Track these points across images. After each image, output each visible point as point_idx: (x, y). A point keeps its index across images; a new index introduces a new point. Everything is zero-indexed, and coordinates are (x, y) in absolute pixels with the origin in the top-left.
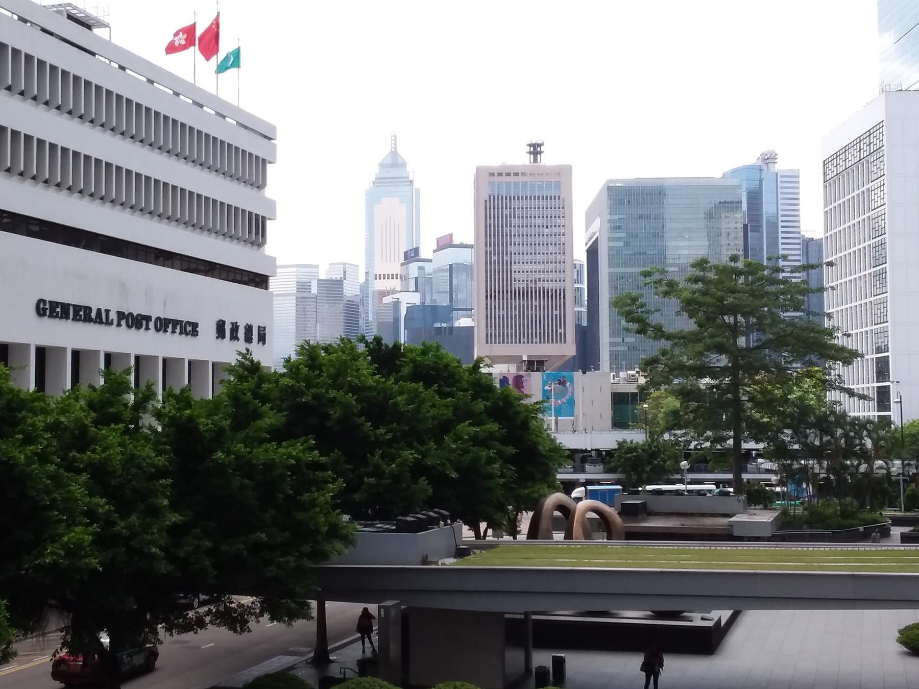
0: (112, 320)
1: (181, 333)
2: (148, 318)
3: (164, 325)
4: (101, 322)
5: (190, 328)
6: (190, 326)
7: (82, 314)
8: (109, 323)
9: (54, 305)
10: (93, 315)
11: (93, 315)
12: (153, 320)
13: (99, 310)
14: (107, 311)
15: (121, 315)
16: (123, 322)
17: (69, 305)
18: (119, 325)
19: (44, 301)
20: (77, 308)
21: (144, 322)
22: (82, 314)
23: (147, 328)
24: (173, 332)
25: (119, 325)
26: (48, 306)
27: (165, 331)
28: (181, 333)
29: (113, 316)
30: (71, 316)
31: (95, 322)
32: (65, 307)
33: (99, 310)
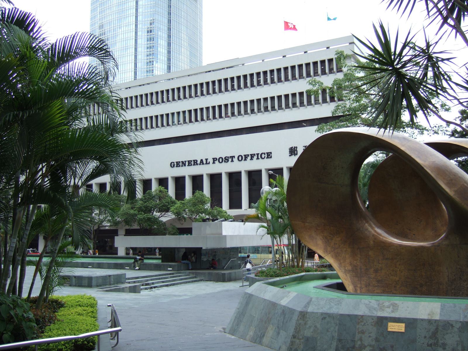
0: (209, 162)
1: (258, 158)
2: (233, 157)
4: (203, 164)
5: (266, 156)
6: (265, 155)
10: (199, 162)
11: (199, 162)
12: (236, 157)
13: (202, 160)
14: (207, 160)
15: (214, 160)
17: (185, 161)
19: (174, 163)
21: (230, 160)
23: (232, 161)
24: (251, 159)
25: (214, 163)
26: (175, 164)
27: (245, 160)
28: (258, 158)
29: (211, 161)
31: (200, 164)
33: (202, 160)
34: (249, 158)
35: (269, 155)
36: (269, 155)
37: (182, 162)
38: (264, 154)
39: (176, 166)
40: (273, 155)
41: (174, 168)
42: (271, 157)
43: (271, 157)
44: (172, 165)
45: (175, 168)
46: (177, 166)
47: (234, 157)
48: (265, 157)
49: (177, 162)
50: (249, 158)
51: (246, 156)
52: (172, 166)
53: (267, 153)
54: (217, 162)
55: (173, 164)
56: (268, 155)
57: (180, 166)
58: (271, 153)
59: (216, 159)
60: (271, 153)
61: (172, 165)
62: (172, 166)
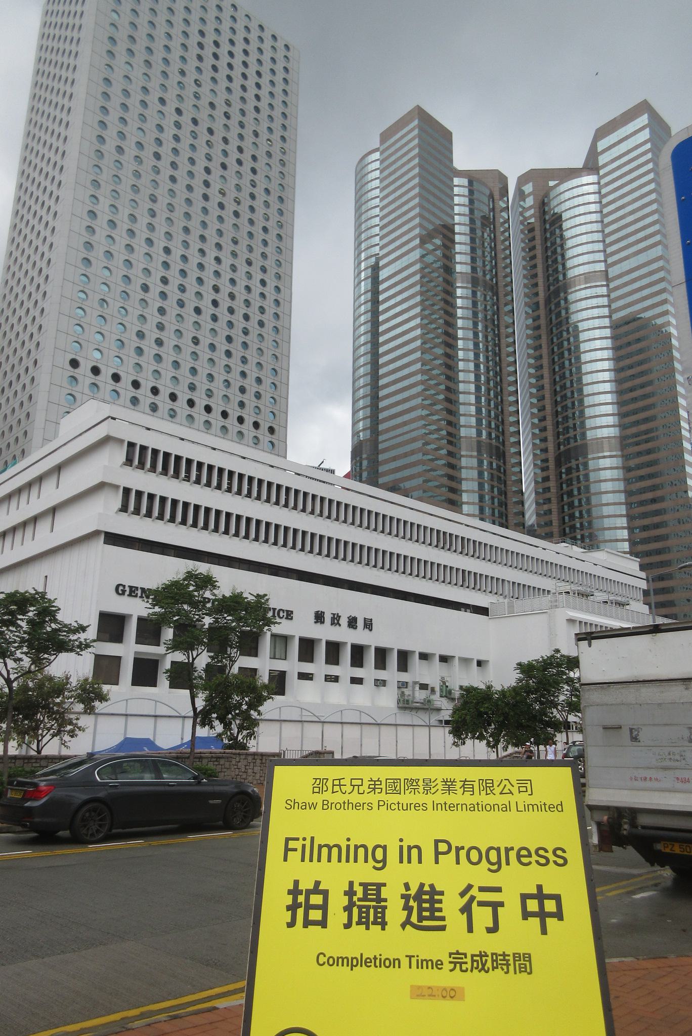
5: (285, 614)
19: (124, 586)
26: (127, 589)
37: (143, 590)
38: (283, 611)
39: (127, 593)
41: (122, 597)
42: (292, 619)
43: (292, 619)
44: (120, 590)
45: (125, 598)
46: (130, 595)
49: (131, 587)
52: (120, 592)
53: (287, 611)
55: (121, 588)
56: (288, 615)
57: (136, 596)
58: (292, 612)
60: (292, 612)
61: (120, 590)
62: (120, 592)
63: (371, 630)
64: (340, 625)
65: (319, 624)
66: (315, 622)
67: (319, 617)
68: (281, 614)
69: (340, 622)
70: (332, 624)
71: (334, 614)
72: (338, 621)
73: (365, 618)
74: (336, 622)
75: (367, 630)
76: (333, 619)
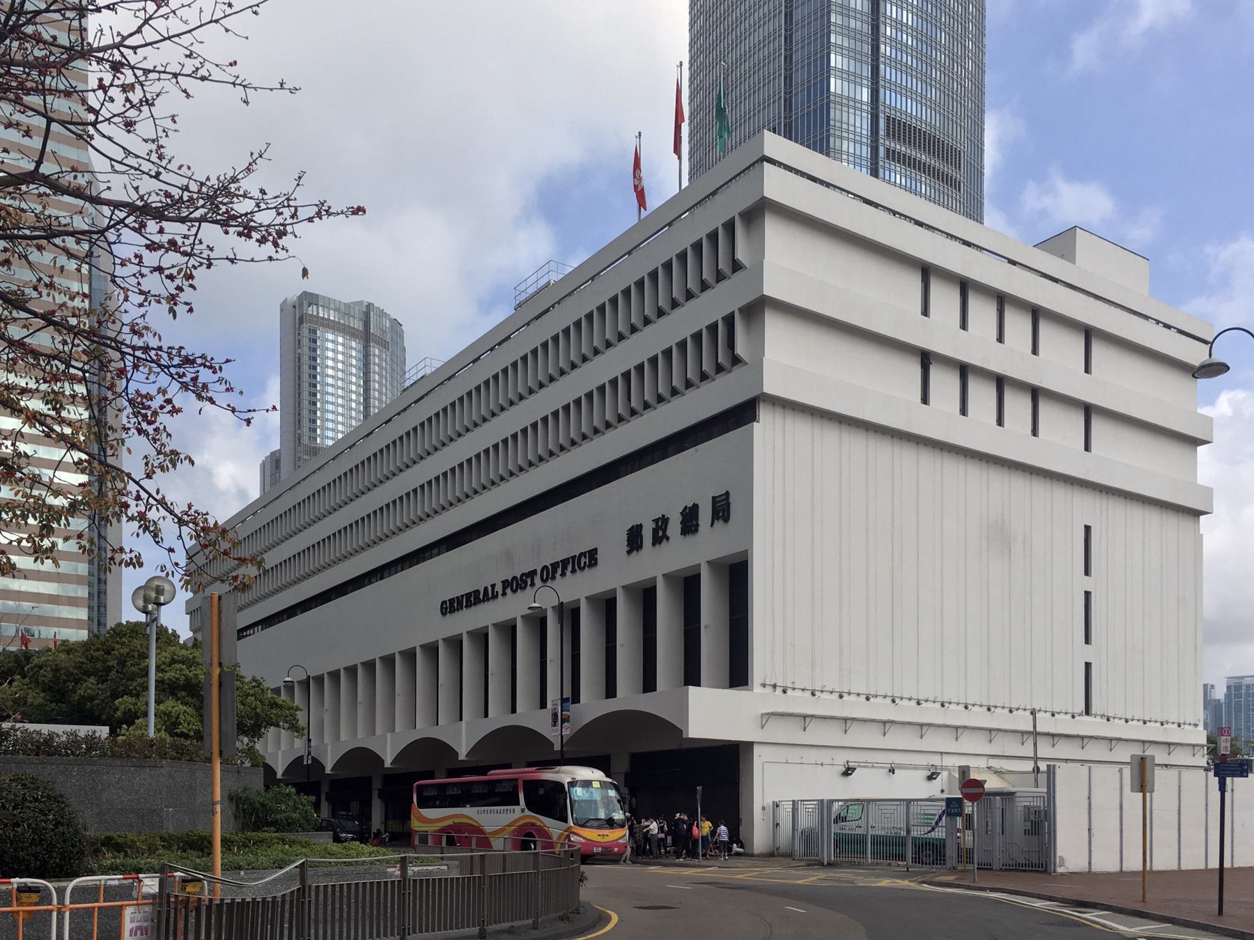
1: (573, 571)
2: (532, 574)
3: (550, 572)
6: (585, 557)
7: (473, 599)
8: (495, 597)
9: (451, 601)
10: (481, 597)
11: (481, 597)
14: (493, 586)
15: (506, 584)
16: (508, 591)
17: (462, 596)
18: (504, 594)
20: (468, 595)
22: (473, 599)
23: (533, 584)
24: (563, 574)
27: (553, 578)
29: (499, 588)
30: (464, 605)
31: (484, 601)
32: (459, 600)
33: (486, 588)
34: (559, 571)
35: (591, 558)
36: (591, 558)
37: (458, 597)
40: (599, 556)
46: (450, 612)
47: (534, 572)
48: (585, 563)
50: (559, 571)
51: (555, 566)
54: (508, 591)
59: (507, 580)
63: (726, 519)
64: (668, 539)
65: (635, 552)
66: (629, 552)
67: (634, 540)
68: (583, 560)
69: (669, 533)
70: (654, 544)
71: (656, 521)
72: (665, 531)
73: (714, 498)
74: (661, 534)
75: (719, 524)
76: (655, 531)
